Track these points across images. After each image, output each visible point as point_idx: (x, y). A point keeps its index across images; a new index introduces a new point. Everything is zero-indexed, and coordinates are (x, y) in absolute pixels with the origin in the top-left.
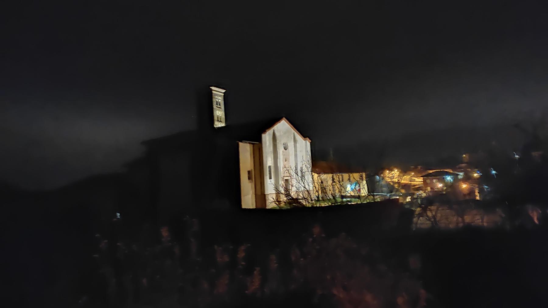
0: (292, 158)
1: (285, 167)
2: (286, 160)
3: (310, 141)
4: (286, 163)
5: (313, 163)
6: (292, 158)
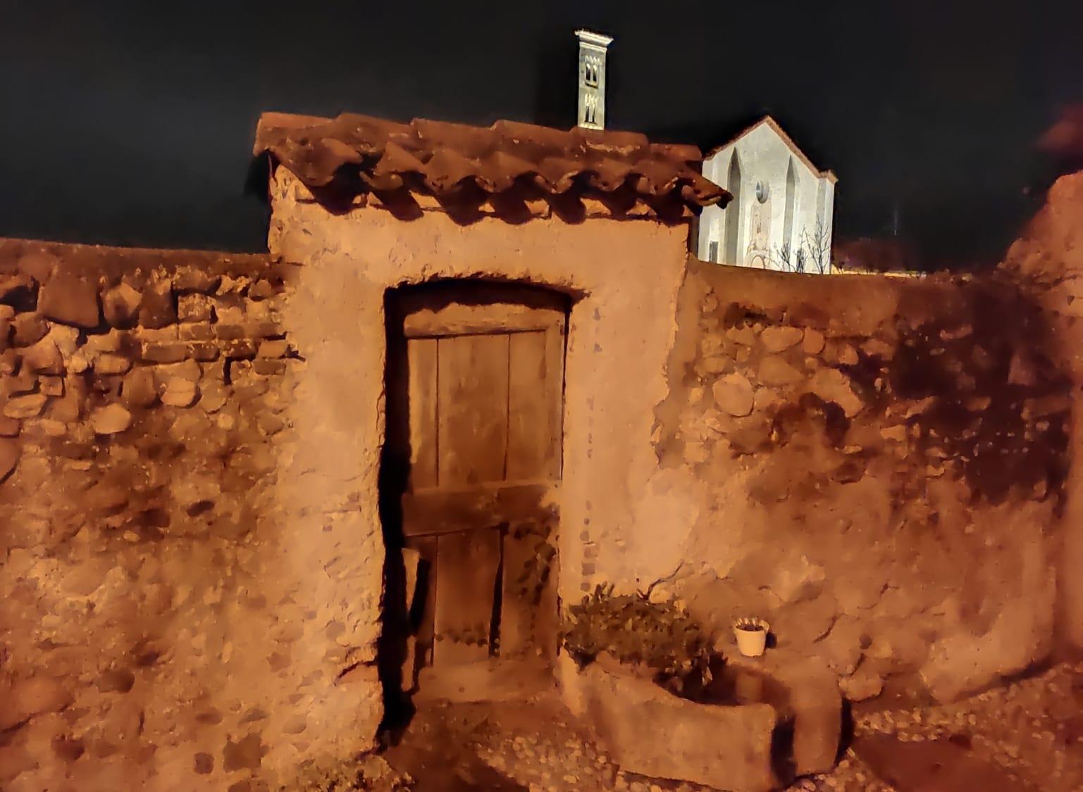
0: (777, 225)
1: (755, 248)
2: (759, 231)
3: (836, 180)
4: (757, 237)
5: (836, 234)
6: (777, 225)
